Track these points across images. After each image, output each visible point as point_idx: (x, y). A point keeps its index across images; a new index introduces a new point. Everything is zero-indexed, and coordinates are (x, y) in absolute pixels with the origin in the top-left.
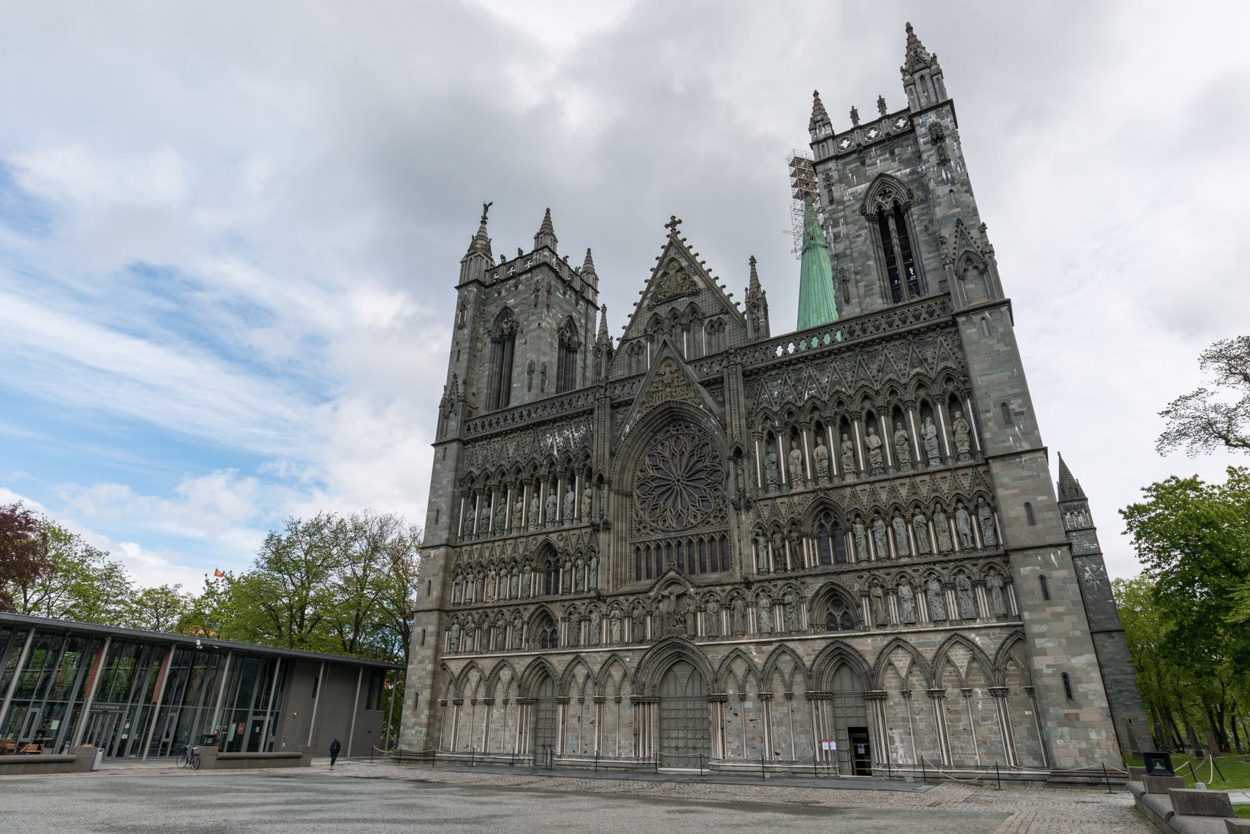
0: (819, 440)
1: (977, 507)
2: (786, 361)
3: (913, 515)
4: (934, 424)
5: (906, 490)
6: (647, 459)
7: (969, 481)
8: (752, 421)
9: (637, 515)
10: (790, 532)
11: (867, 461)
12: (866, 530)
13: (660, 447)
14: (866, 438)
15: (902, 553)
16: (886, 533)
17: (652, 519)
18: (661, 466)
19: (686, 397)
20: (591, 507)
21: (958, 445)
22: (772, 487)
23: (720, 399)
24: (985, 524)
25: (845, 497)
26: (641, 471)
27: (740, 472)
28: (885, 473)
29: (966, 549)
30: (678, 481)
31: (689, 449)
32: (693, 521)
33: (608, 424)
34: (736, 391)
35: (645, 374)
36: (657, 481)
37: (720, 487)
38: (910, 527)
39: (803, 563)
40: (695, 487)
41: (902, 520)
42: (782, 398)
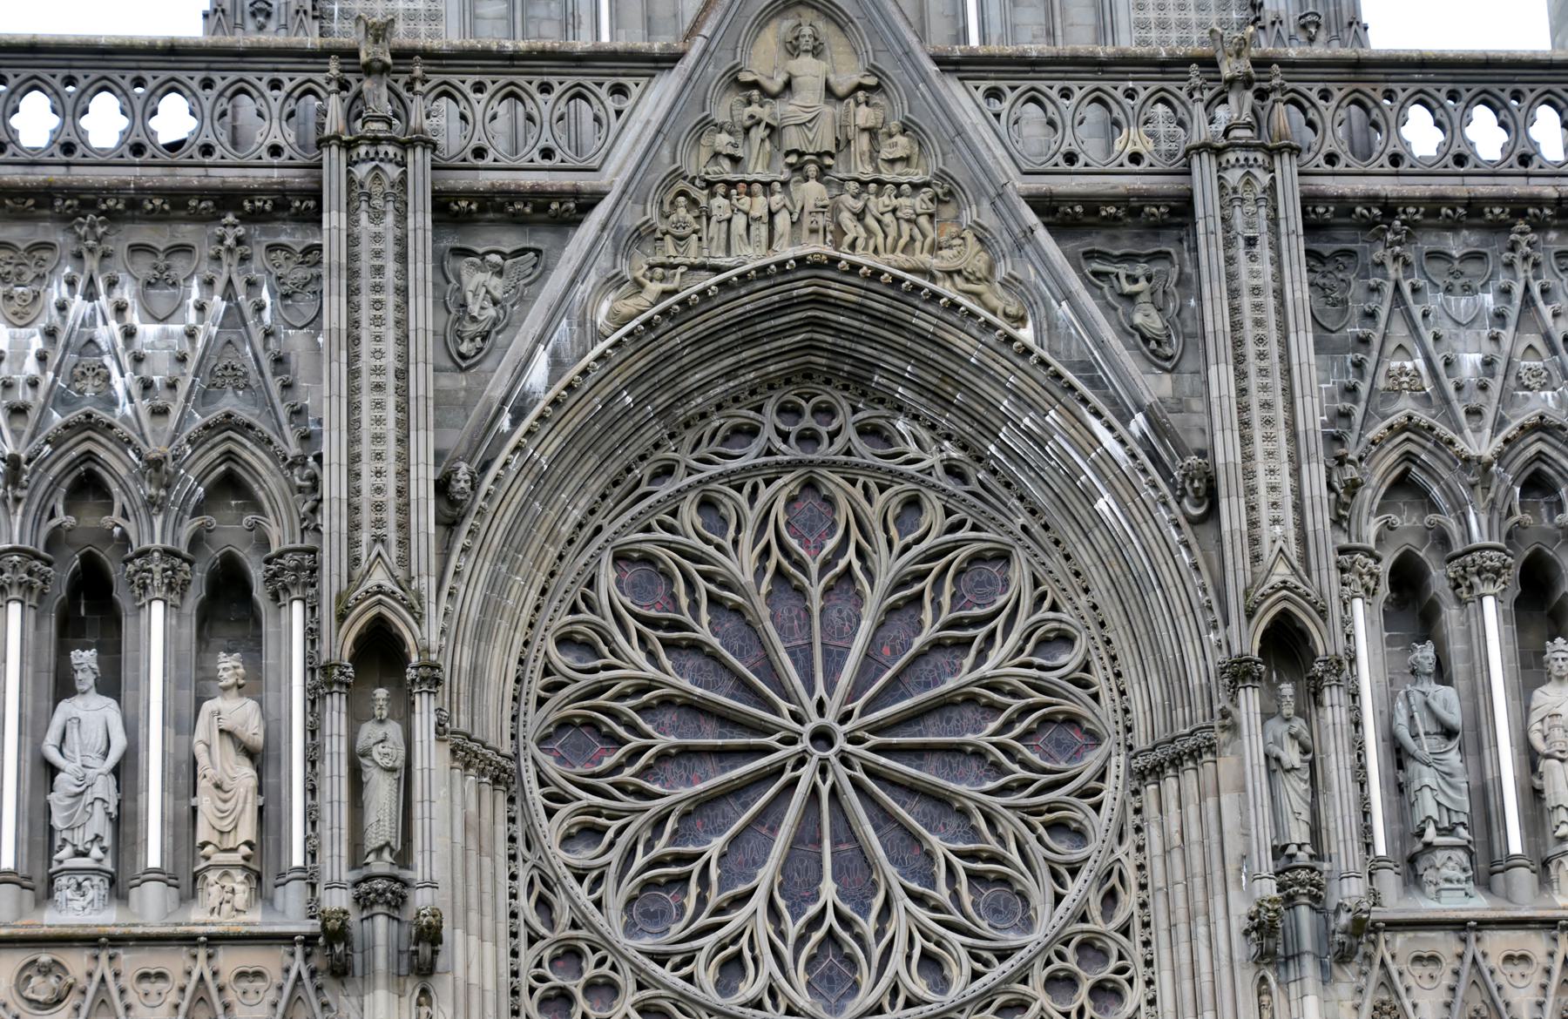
2: (1538, 201)
6: (607, 576)
8: (1353, 487)
9: (543, 905)
13: (689, 514)
17: (647, 943)
18: (704, 633)
19: (923, 258)
20: (268, 817)
22: (1449, 865)
23: (1147, 318)
26: (565, 641)
27: (1292, 755)
30: (823, 737)
31: (888, 567)
32: (920, 987)
33: (423, 313)
34: (1270, 302)
35: (669, 60)
36: (669, 717)
37: (1081, 812)
40: (910, 789)
42: (1506, 399)
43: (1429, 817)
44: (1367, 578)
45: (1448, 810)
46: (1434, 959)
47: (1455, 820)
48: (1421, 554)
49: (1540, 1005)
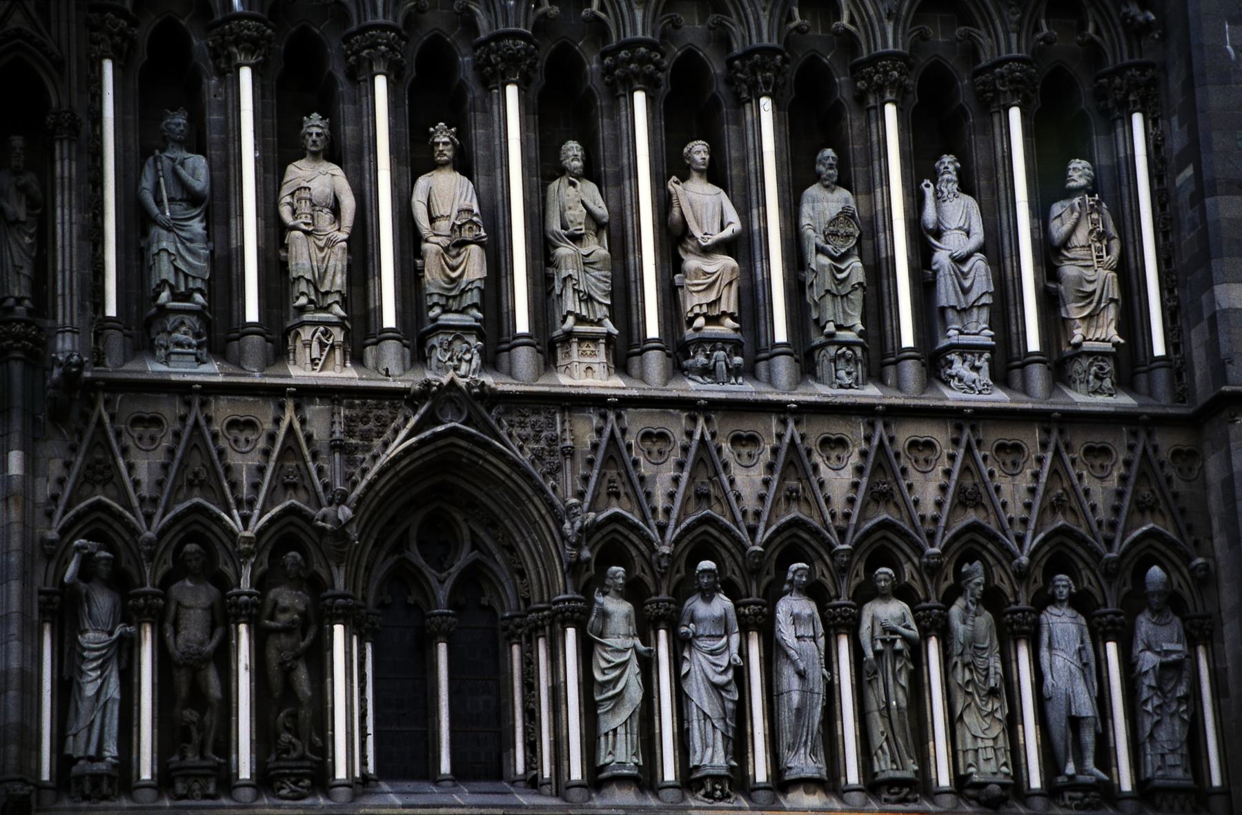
0: (443, 137)
1: (1136, 600)
3: (868, 592)
4: (966, 186)
5: (847, 475)
7: (1113, 483)
10: (261, 583)
11: (670, 297)
12: (645, 627)
14: (673, 185)
15: (803, 763)
16: (743, 652)
21: (1074, 311)
24: (1159, 688)
25: (569, 453)
28: (749, 372)
29: (1073, 784)
38: (844, 644)
39: (325, 750)
41: (805, 607)
43: (165, 282)
44: (118, 39)
45: (186, 276)
46: (156, 421)
47: (191, 285)
48: (183, 23)
49: (261, 470)
